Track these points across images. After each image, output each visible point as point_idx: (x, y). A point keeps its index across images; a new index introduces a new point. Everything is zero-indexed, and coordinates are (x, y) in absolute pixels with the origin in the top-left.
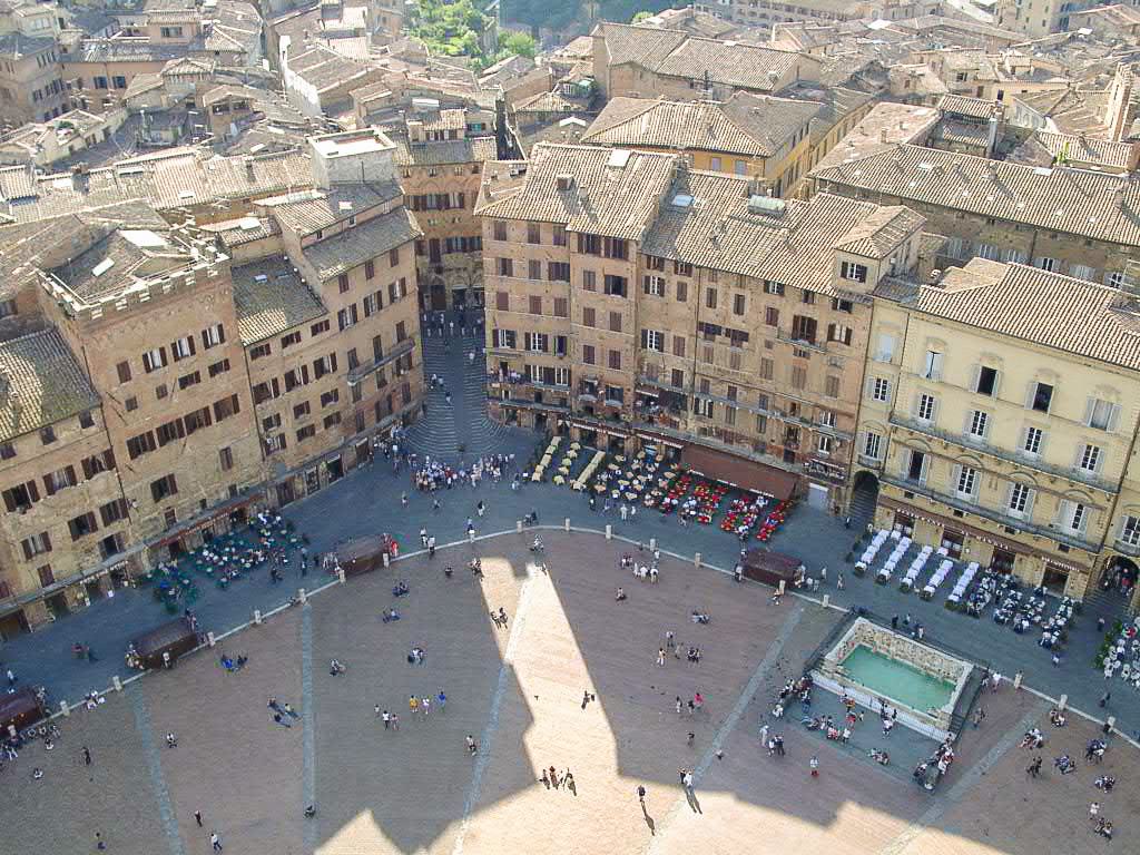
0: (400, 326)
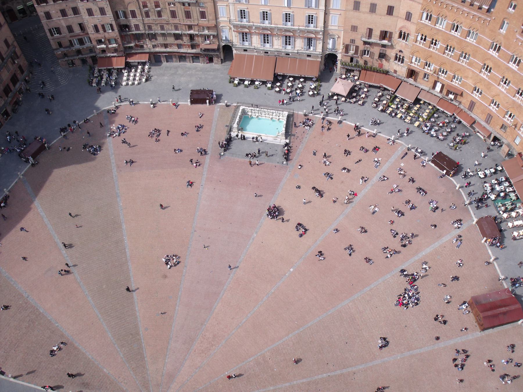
0: (6, 42)
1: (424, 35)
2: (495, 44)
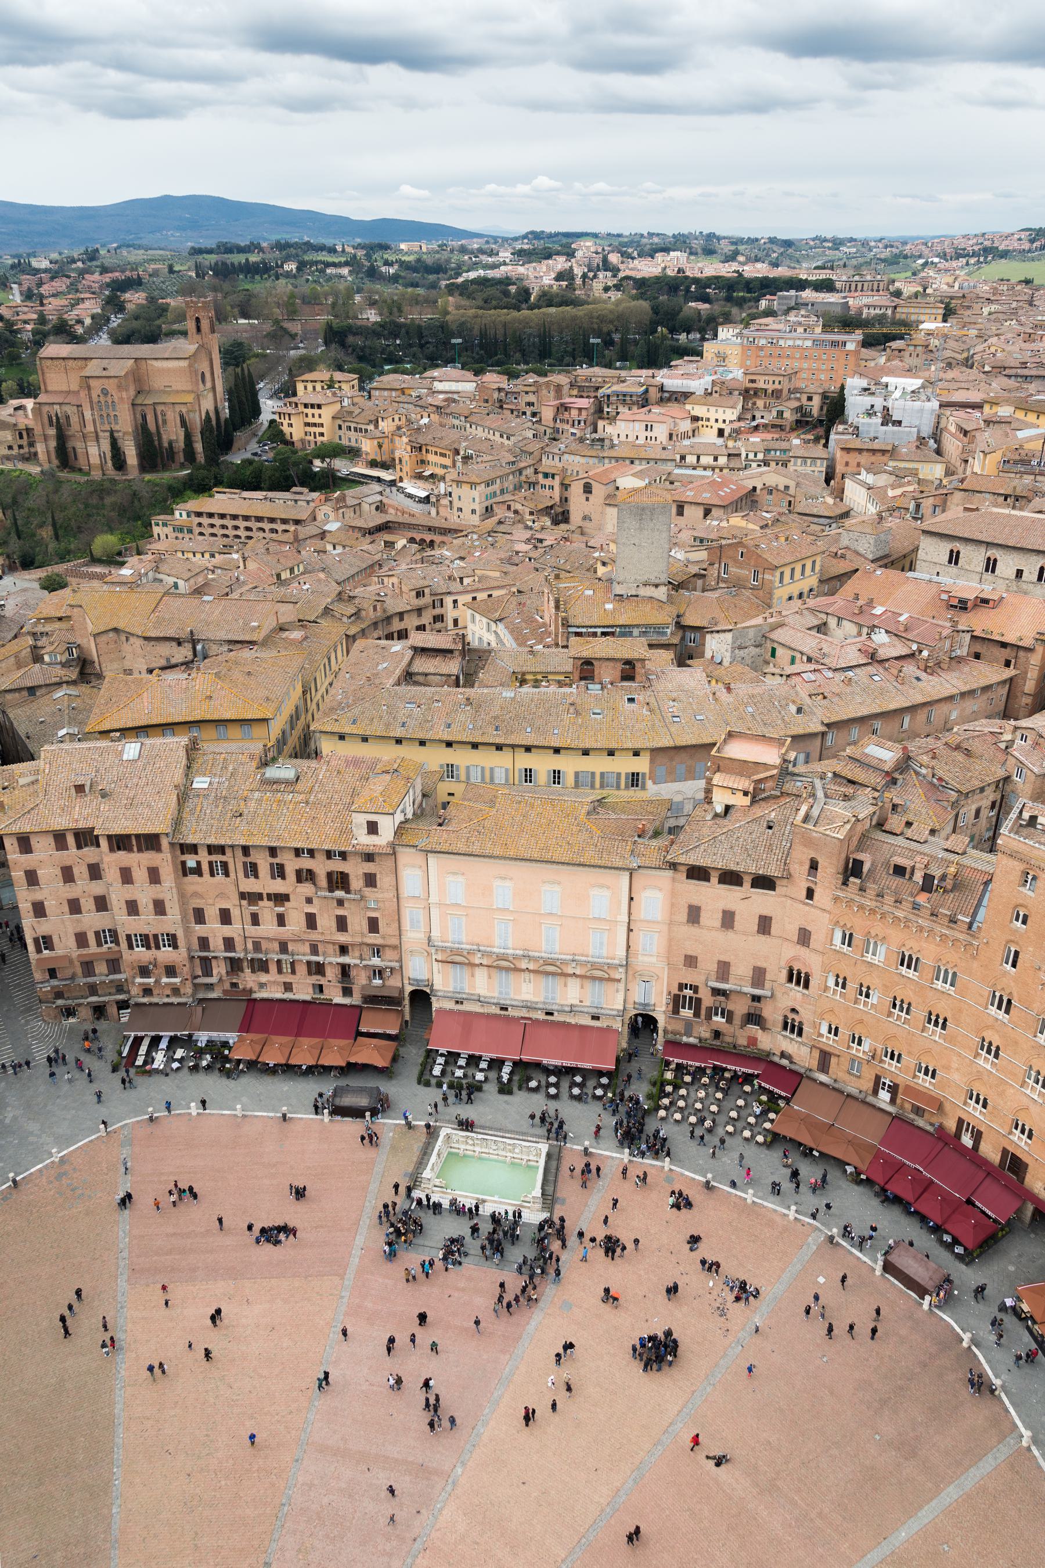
1: (841, 976)
2: (998, 994)
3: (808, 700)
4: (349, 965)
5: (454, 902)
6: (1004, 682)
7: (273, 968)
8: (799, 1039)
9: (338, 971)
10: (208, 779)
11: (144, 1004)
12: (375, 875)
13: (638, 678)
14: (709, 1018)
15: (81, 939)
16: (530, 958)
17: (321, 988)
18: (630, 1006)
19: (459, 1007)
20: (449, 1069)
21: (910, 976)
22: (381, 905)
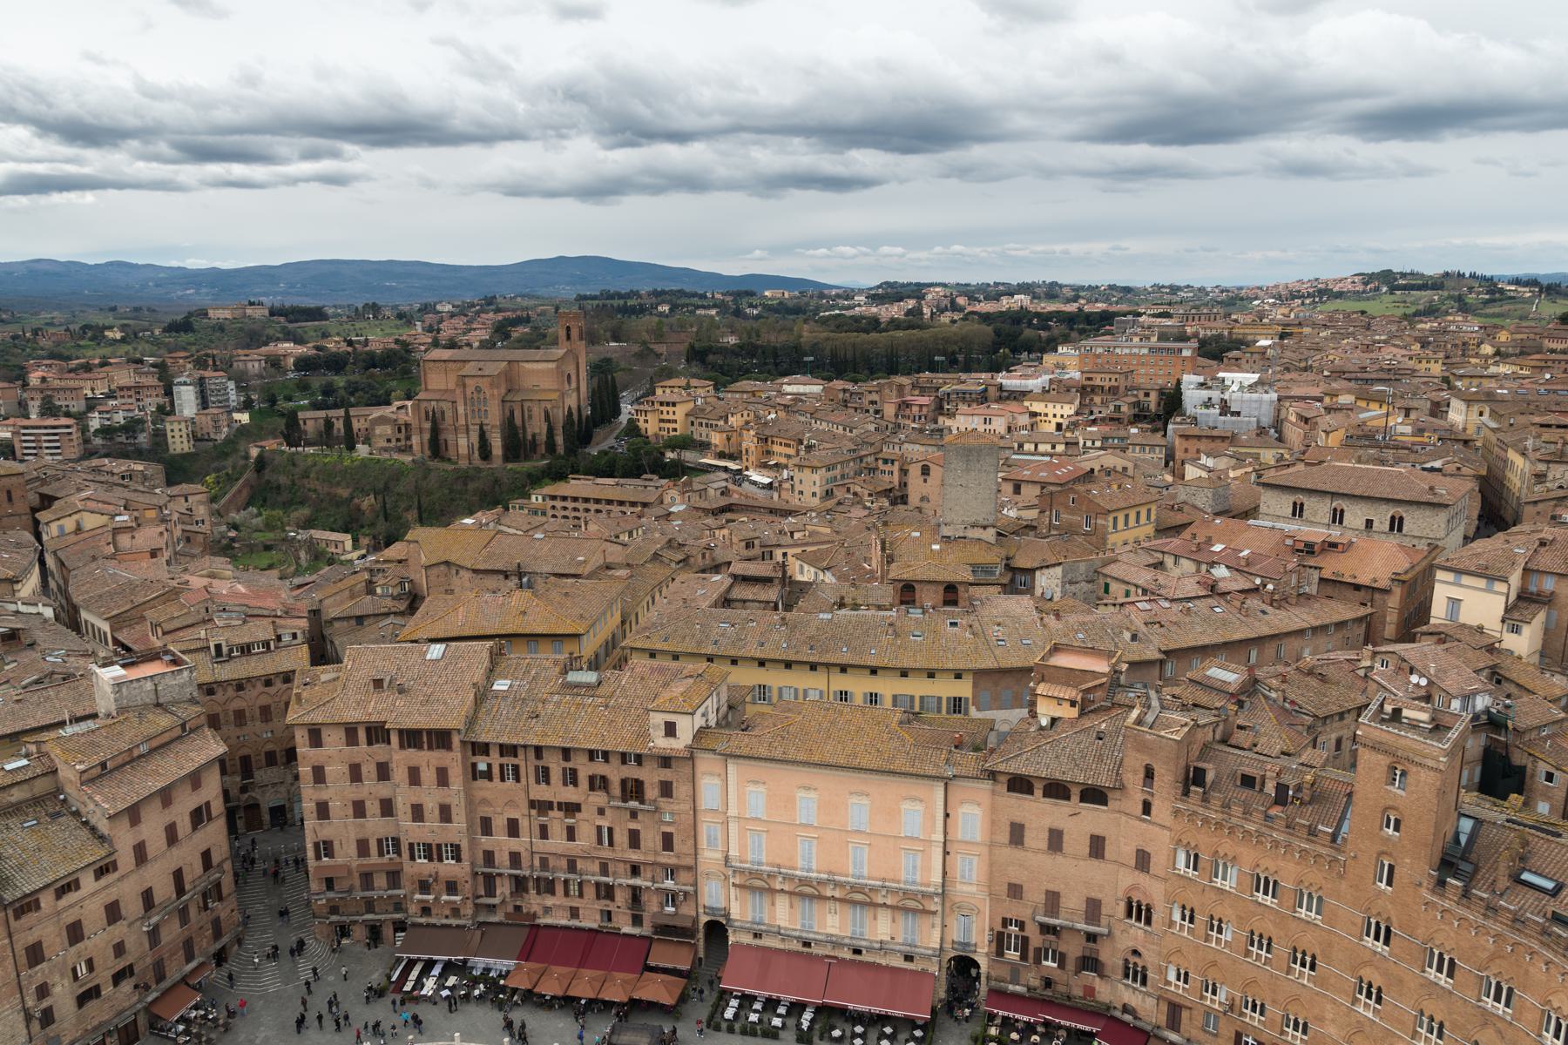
2: (1373, 921)
3: (1144, 629)
4: (640, 888)
5: (753, 815)
6: (1360, 620)
7: (559, 889)
8: (1143, 989)
9: (628, 894)
10: (509, 682)
11: (421, 925)
12: (671, 783)
13: (961, 602)
14: (1038, 961)
15: (363, 847)
16: (837, 884)
17: (608, 915)
18: (948, 946)
19: (758, 942)
20: (742, 1013)
21: (1268, 903)
22: (676, 817)
